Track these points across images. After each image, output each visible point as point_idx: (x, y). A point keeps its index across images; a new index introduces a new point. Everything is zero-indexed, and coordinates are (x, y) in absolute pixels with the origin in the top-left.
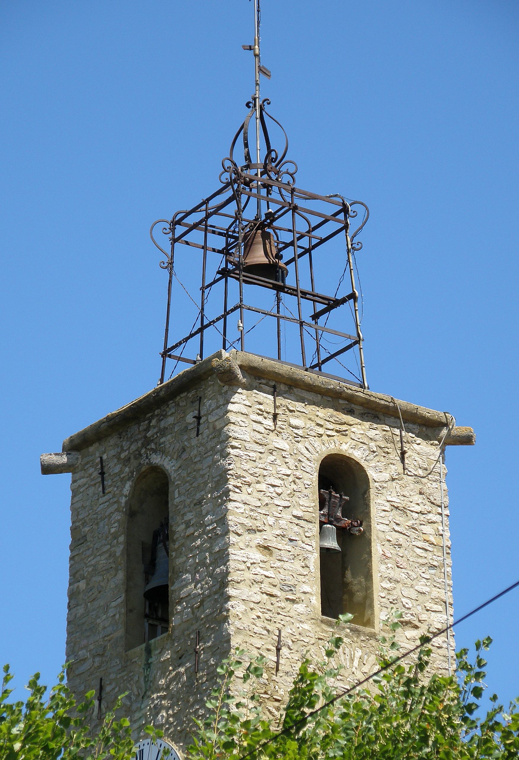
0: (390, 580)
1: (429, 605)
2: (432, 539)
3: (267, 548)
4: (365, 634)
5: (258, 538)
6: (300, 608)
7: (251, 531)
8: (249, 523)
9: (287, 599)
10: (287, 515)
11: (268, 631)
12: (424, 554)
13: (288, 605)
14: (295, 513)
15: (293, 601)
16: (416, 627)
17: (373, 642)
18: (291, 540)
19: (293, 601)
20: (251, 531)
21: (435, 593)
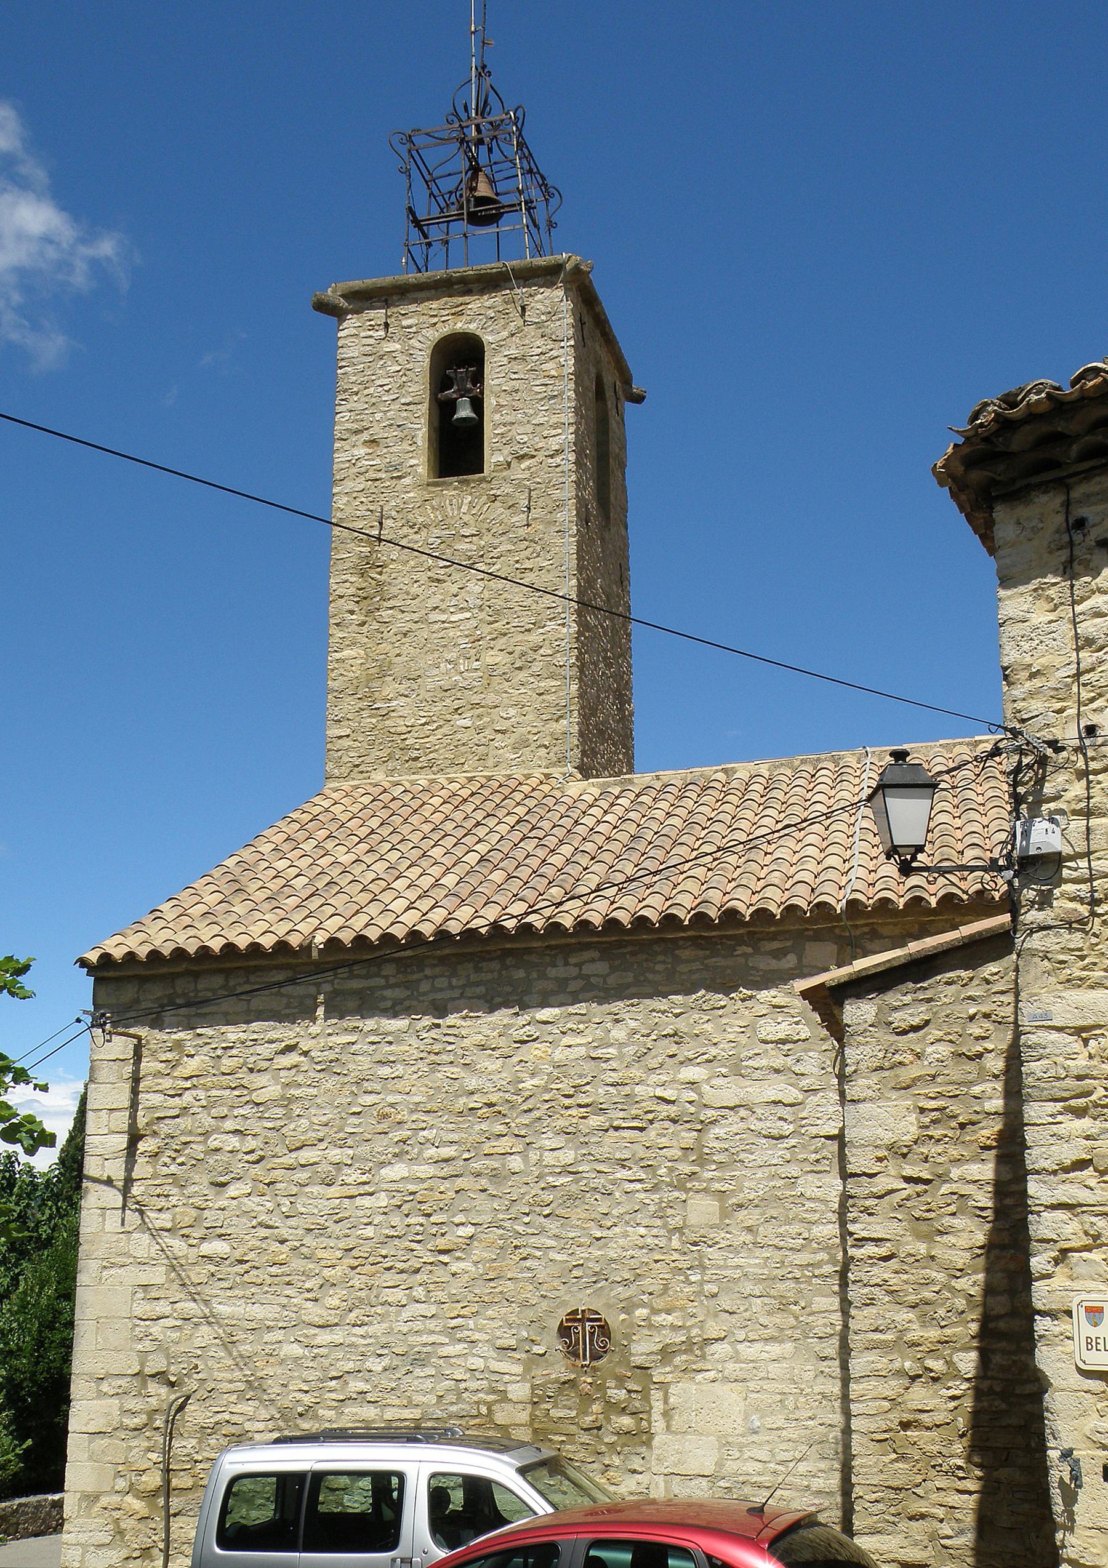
0: (504, 425)
1: (545, 433)
2: (553, 373)
3: (374, 441)
4: (474, 481)
5: (365, 436)
6: (407, 481)
7: (357, 432)
8: (355, 426)
9: (392, 478)
10: (396, 406)
11: (371, 511)
12: (544, 388)
13: (394, 482)
14: (403, 401)
15: (400, 478)
16: (533, 457)
17: (484, 485)
18: (399, 426)
19: (400, 478)
20: (357, 432)
21: (554, 419)
